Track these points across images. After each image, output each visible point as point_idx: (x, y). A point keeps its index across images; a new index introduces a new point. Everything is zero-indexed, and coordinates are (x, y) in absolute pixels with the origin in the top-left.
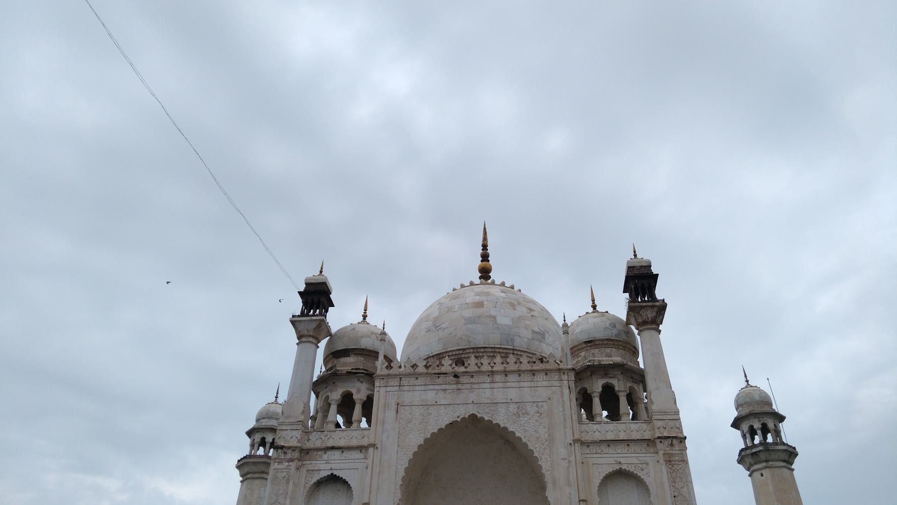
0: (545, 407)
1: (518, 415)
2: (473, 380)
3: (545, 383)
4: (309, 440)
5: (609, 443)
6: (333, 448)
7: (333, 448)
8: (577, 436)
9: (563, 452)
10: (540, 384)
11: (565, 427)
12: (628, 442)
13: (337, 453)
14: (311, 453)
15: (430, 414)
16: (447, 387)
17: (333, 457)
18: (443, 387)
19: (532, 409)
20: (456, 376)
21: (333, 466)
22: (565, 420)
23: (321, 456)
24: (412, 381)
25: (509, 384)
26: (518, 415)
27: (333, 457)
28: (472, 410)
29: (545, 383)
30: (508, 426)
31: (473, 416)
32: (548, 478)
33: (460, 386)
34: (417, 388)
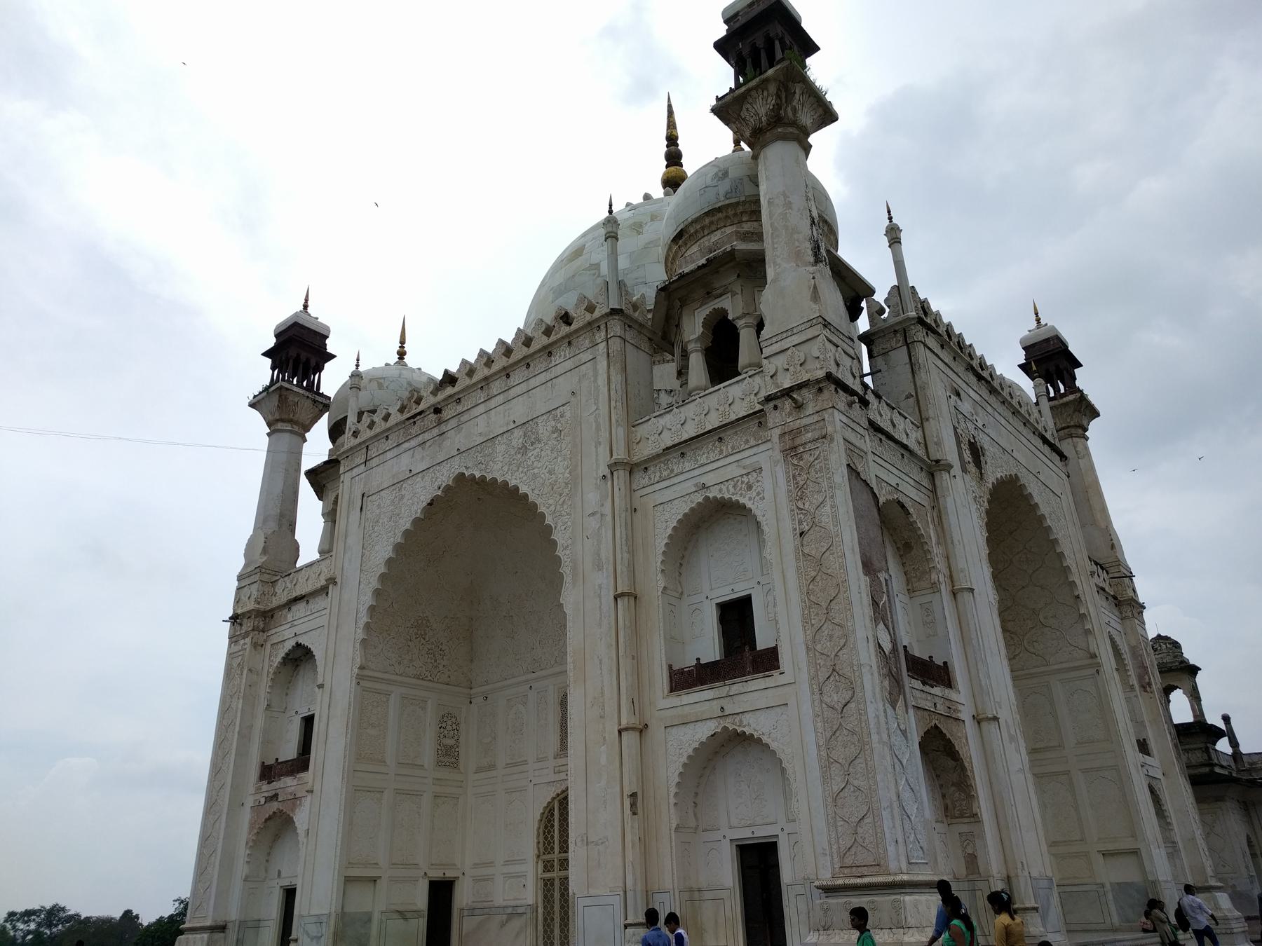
0: (568, 415)
1: (524, 449)
2: (460, 408)
3: (569, 364)
4: (275, 594)
5: (681, 448)
6: (297, 600)
7: (297, 600)
8: (620, 454)
9: (592, 497)
10: (559, 370)
11: (598, 444)
12: (717, 434)
13: (300, 608)
14: (278, 614)
15: (403, 496)
16: (427, 436)
17: (298, 615)
18: (420, 439)
19: (544, 428)
20: (437, 411)
21: (297, 630)
22: (598, 429)
23: (286, 617)
24: (385, 445)
25: (513, 392)
26: (524, 449)
27: (298, 615)
28: (457, 467)
29: (569, 364)
30: (508, 478)
31: (460, 477)
32: (566, 569)
33: (444, 428)
34: (389, 455)
